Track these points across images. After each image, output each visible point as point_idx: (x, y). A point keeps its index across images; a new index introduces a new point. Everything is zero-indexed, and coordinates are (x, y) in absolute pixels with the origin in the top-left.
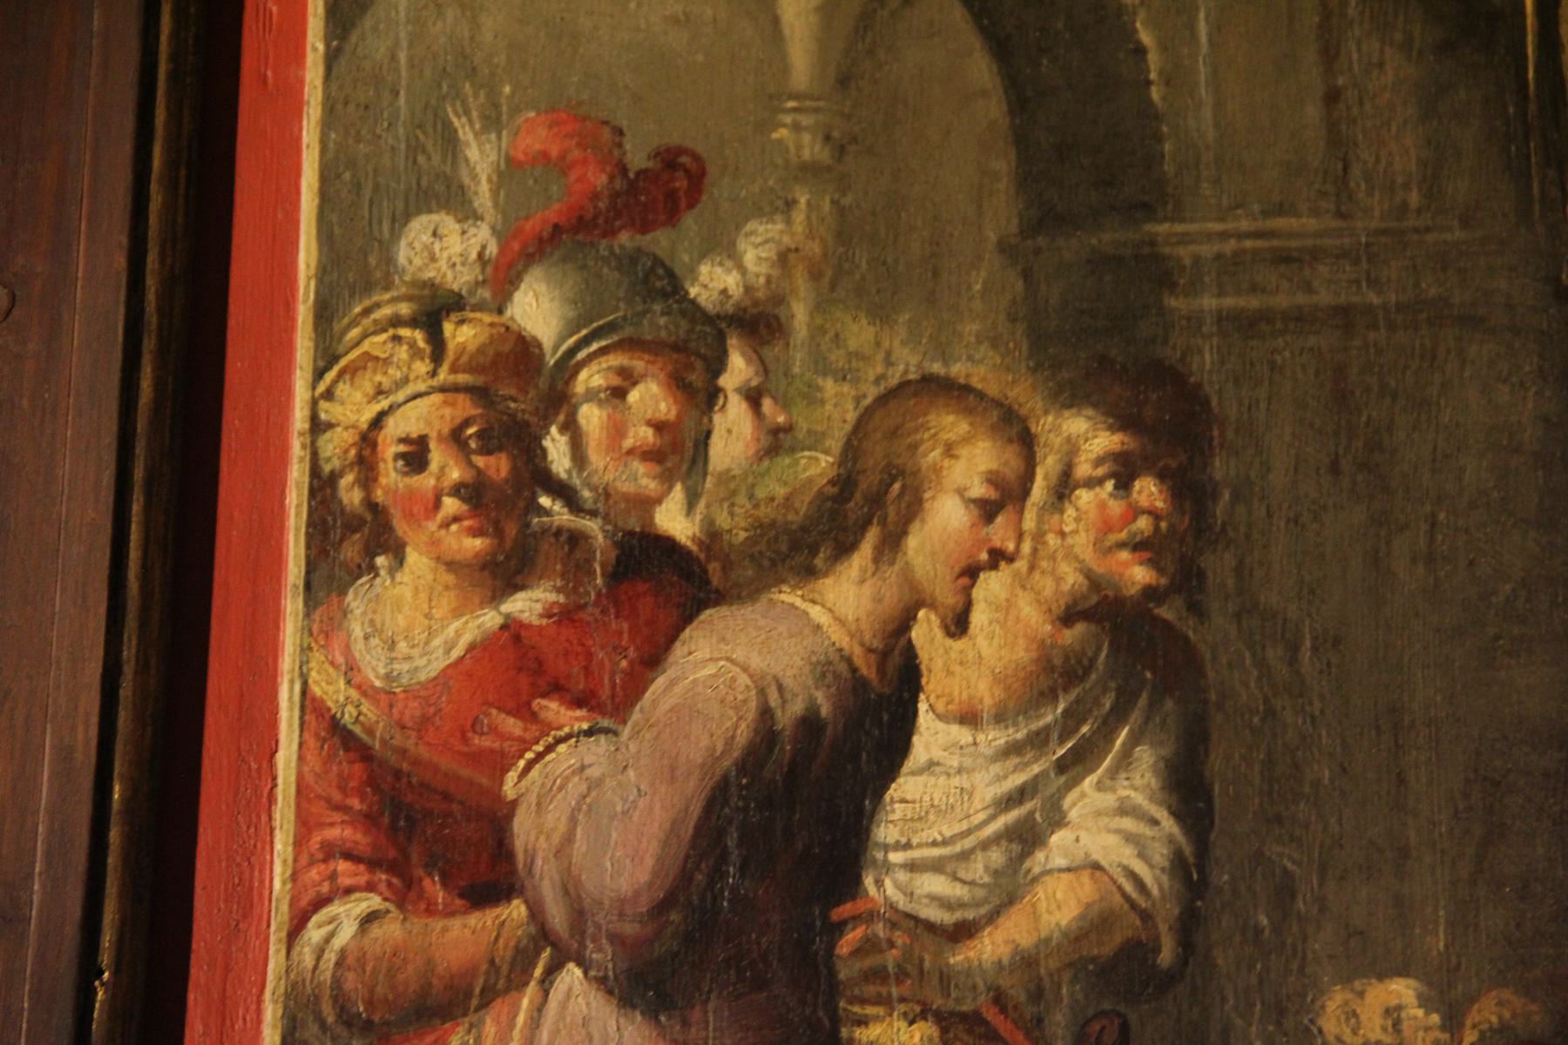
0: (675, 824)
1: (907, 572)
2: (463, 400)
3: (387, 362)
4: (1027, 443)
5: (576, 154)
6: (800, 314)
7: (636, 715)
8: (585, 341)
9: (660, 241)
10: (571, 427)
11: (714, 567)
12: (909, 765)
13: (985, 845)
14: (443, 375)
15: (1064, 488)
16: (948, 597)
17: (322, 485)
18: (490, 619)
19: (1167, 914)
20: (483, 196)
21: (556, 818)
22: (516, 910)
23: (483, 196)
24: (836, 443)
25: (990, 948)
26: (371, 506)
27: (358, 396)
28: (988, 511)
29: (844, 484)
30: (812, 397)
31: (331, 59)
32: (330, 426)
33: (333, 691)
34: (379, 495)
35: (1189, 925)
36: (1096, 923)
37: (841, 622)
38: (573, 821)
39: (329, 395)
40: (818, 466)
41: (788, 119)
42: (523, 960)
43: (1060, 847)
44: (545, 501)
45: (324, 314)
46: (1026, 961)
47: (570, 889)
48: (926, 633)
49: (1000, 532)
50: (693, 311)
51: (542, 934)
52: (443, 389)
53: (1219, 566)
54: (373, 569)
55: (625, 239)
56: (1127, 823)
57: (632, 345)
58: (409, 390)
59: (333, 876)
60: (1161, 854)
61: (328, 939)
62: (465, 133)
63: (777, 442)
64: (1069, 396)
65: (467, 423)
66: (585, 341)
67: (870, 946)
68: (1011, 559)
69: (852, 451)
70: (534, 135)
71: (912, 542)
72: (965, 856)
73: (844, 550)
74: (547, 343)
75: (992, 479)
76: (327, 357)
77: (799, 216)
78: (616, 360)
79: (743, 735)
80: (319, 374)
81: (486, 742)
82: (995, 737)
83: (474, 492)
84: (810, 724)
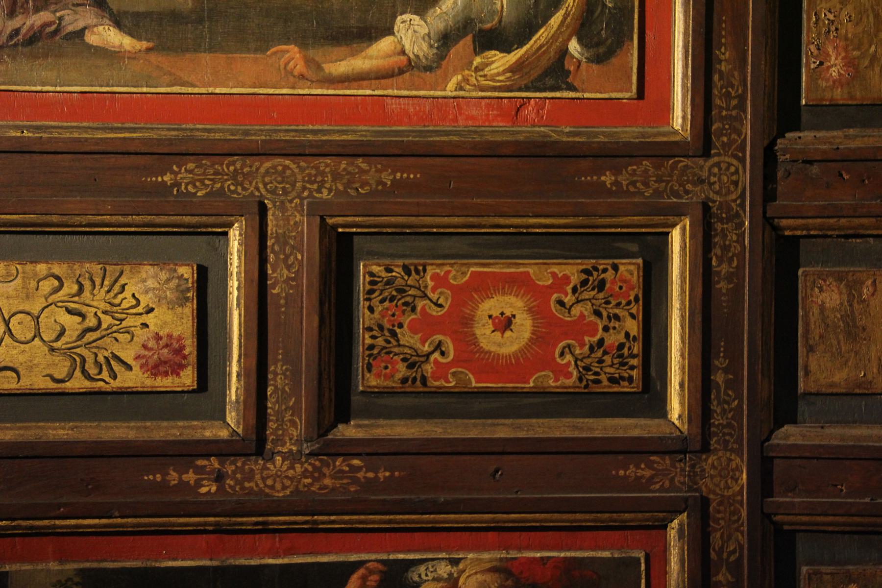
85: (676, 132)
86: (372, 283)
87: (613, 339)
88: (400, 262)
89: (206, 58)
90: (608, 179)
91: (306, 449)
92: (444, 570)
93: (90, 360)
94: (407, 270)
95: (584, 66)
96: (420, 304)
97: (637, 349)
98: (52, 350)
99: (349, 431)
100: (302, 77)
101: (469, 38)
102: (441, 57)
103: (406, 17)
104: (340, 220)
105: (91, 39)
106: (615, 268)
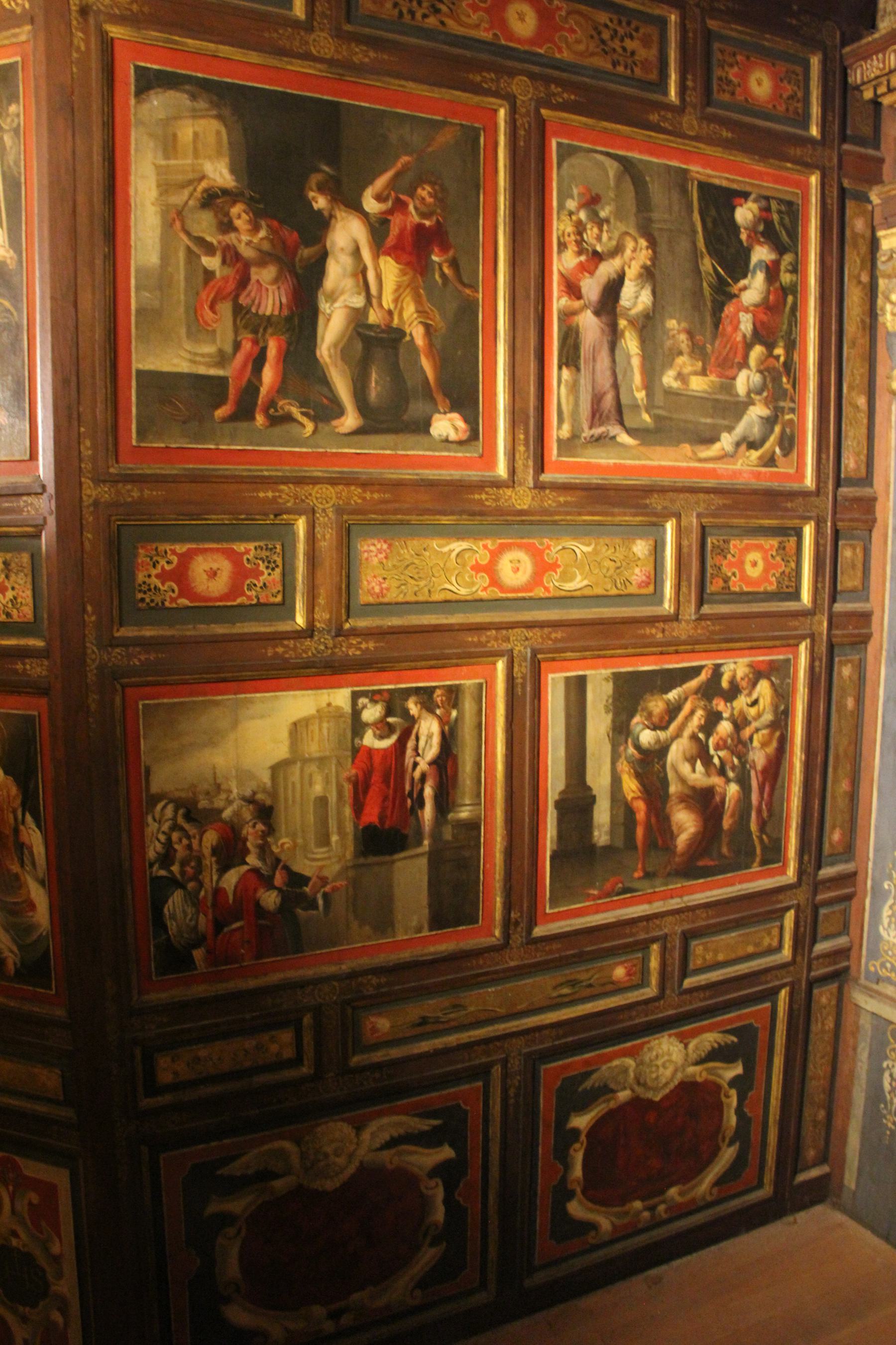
6: (612, 220)
15: (641, 249)
22: (582, 302)
23: (576, 197)
35: (654, 311)
36: (644, 310)
40: (614, 243)
45: (558, 213)
48: (626, 268)
49: (634, 255)
53: (657, 262)
63: (610, 239)
76: (558, 218)
83: (576, 241)
84: (614, 279)
85: (808, 487)
87: (787, 570)
88: (722, 538)
91: (693, 617)
92: (732, 666)
93: (618, 581)
94: (724, 541)
96: (729, 556)
97: (794, 574)
98: (605, 577)
99: (706, 609)
100: (690, 458)
102: (736, 452)
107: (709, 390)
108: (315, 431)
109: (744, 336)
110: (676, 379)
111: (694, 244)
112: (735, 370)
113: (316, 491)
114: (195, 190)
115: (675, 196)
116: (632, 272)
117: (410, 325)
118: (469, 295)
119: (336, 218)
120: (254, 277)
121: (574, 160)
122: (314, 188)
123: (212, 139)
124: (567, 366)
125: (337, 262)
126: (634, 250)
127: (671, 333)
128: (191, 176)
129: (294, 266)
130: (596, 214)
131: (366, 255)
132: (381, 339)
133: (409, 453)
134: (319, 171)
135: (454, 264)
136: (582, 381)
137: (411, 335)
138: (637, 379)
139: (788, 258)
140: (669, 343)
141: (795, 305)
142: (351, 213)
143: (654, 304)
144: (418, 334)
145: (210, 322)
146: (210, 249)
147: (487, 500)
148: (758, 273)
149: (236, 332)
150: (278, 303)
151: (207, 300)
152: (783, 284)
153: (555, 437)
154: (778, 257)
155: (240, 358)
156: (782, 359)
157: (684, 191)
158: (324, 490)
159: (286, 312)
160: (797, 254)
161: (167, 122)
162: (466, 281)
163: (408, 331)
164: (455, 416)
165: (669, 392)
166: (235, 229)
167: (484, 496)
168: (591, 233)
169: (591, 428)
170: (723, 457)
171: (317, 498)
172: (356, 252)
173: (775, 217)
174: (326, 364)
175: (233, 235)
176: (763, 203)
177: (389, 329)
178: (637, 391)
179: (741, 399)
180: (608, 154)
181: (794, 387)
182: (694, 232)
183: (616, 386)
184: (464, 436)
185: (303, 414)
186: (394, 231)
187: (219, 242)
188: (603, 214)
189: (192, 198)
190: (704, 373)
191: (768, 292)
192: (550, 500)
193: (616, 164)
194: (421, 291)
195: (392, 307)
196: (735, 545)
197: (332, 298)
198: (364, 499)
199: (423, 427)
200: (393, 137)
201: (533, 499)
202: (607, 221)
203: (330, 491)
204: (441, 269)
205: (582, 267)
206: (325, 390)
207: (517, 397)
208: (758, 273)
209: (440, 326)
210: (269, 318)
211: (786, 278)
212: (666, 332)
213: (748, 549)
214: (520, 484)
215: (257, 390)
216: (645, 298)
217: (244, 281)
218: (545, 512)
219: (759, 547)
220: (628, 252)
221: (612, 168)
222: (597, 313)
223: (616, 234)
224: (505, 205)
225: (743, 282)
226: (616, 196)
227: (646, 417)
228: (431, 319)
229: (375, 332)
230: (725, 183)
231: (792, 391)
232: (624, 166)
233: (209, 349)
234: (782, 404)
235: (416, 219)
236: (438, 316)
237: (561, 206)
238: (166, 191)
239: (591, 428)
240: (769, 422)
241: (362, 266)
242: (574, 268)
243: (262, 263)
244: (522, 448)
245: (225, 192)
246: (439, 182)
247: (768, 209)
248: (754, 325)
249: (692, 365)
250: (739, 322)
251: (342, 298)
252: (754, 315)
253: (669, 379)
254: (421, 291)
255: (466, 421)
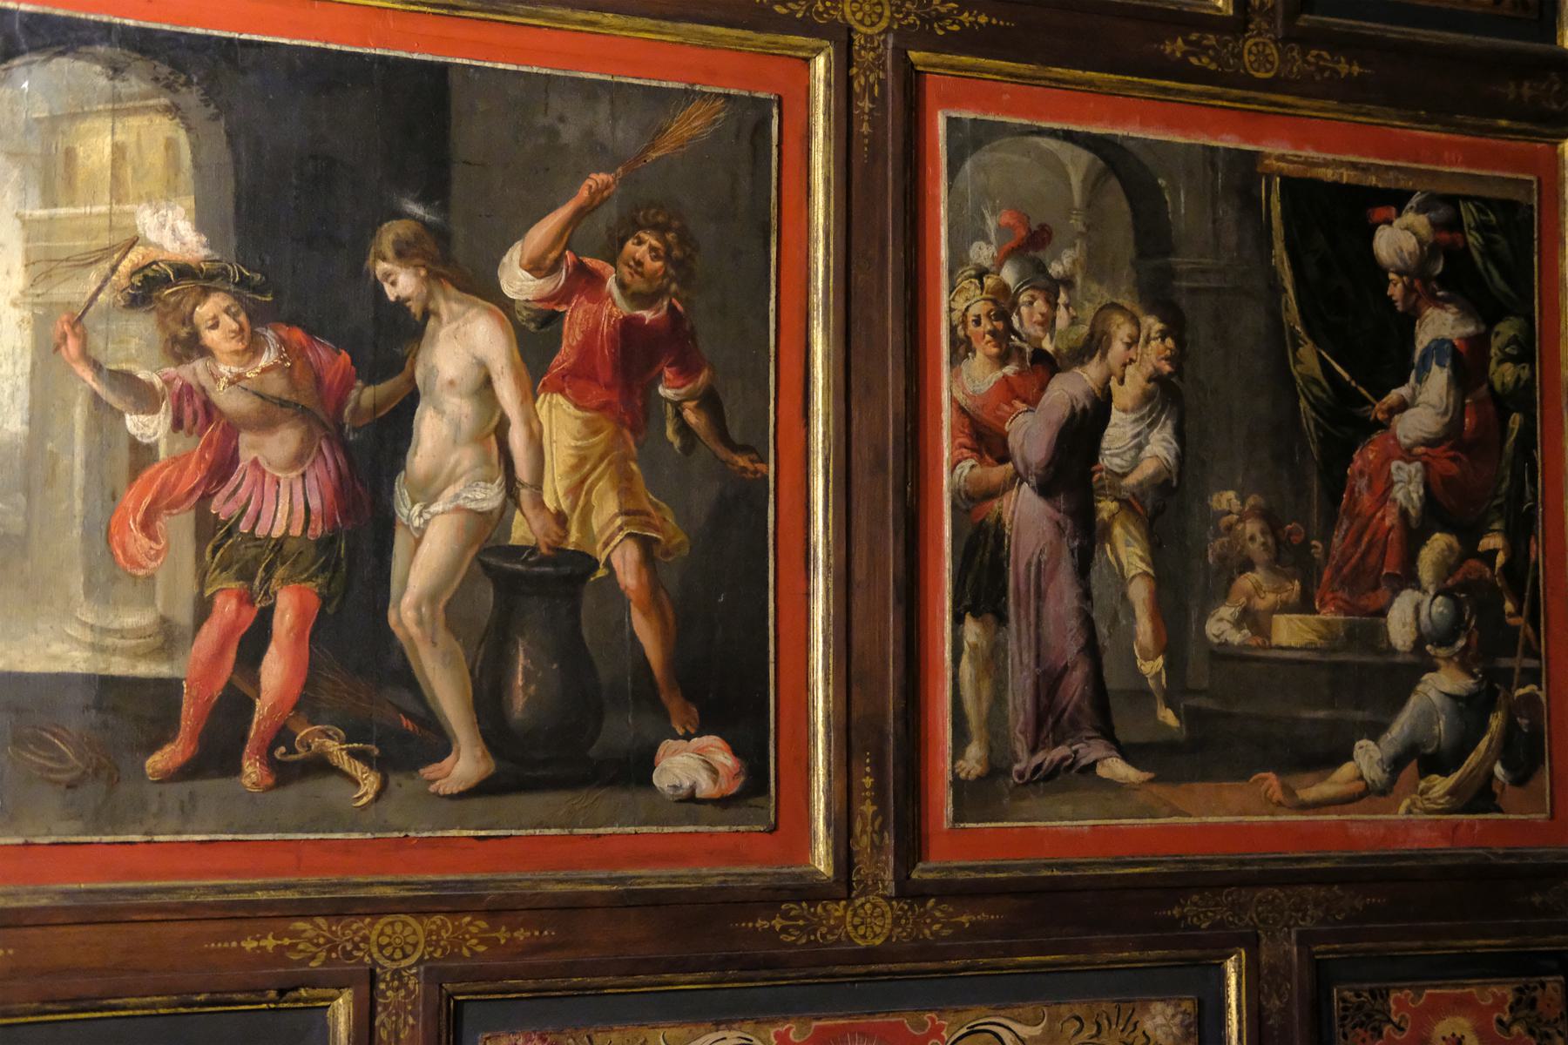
0: (1050, 442)
1: (1108, 365)
2: (990, 303)
3: (969, 289)
4: (1138, 325)
5: (1018, 224)
6: (1078, 280)
7: (1039, 406)
8: (1022, 286)
9: (1041, 254)
10: (1019, 314)
11: (1058, 360)
12: (1110, 424)
13: (1129, 449)
14: (984, 295)
15: (1147, 341)
16: (1119, 373)
17: (953, 330)
18: (999, 374)
19: (1174, 471)
20: (993, 237)
21: (1019, 437)
22: (1010, 465)
23: (993, 237)
24: (1089, 323)
25: (1131, 480)
26: (966, 335)
27: (962, 301)
28: (1129, 346)
29: (1091, 335)
30: (1082, 307)
31: (950, 188)
32: (954, 310)
33: (960, 396)
34: (968, 333)
35: (1180, 475)
36: (1157, 474)
37: (1091, 379)
38: (1024, 439)
39: (953, 300)
40: (1084, 330)
41: (1074, 217)
42: (1013, 480)
43: (1148, 450)
44: (1013, 337)
45: (951, 272)
46: (1140, 484)
47: (1024, 460)
48: (1113, 383)
50: (1050, 278)
51: (1017, 474)
52: (984, 299)
54: (968, 357)
55: (1031, 253)
56: (1164, 444)
57: (1033, 288)
58: (975, 299)
59: (962, 453)
60: (1173, 452)
61: (961, 473)
62: (987, 216)
63: (1074, 321)
64: (1150, 311)
65: (991, 310)
66: (1022, 286)
67: (1101, 479)
68: (1134, 361)
69: (1093, 326)
70: (1006, 218)
71: (1109, 355)
72: (1124, 452)
73: (1092, 357)
74: (1012, 287)
75: (1130, 337)
76: (952, 289)
77: (1078, 249)
78: (1030, 292)
79: (1067, 414)
80: (951, 293)
81: (999, 413)
82: (1132, 417)
83: (993, 333)
84: (1084, 409)
86: (1345, 1009)
88: (1367, 986)
89: (1198, 787)
90: (1537, 899)
94: (1372, 992)
95: (1508, 788)
96: (1387, 1029)
100: (1279, 804)
101: (1415, 762)
102: (1392, 781)
103: (1363, 742)
104: (1322, 947)
105: (1102, 771)
106: (1543, 985)
107: (1320, 643)
108: (379, 796)
109: (1404, 513)
110: (1238, 624)
111: (1275, 316)
112: (1384, 593)
113: (378, 930)
114: (114, 269)
115: (1228, 212)
116: (1126, 394)
117: (606, 544)
118: (744, 469)
119: (437, 315)
120: (246, 456)
121: (985, 156)
122: (390, 254)
123: (155, 157)
124: (976, 615)
125: (440, 412)
126: (1132, 343)
127: (1225, 520)
128: (104, 241)
129: (341, 428)
130: (1041, 268)
131: (507, 392)
132: (541, 577)
133: (601, 831)
134: (399, 215)
135: (710, 402)
136: (1012, 646)
137: (608, 563)
138: (1144, 628)
139: (1507, 329)
140: (1214, 548)
141: (1528, 433)
142: (474, 304)
143: (1181, 458)
144: (625, 564)
145: (141, 558)
146: (145, 398)
147: (784, 929)
148: (1435, 368)
149: (202, 577)
150: (300, 508)
151: (136, 510)
152: (1498, 386)
153: (950, 778)
154: (1483, 328)
155: (210, 633)
156: (1500, 559)
157: (1249, 200)
158: (398, 927)
159: (317, 529)
160: (1530, 319)
161: (54, 122)
162: (735, 434)
163: (602, 558)
164: (711, 741)
165: (1222, 655)
166: (206, 352)
167: (778, 923)
168: (1029, 314)
169: (1033, 751)
170: (1367, 793)
171: (381, 948)
172: (485, 387)
173: (1474, 239)
174: (411, 639)
175: (199, 365)
176: (1443, 212)
177: (560, 554)
178: (1146, 659)
179: (1399, 659)
180: (1068, 136)
181: (1534, 619)
182: (1276, 289)
183: (1092, 649)
184: (729, 786)
185: (353, 754)
186: (572, 336)
187: (168, 382)
188: (1056, 269)
189: (107, 289)
190: (1305, 605)
191: (1460, 411)
192: (938, 921)
193: (1084, 156)
194: (634, 467)
195: (565, 505)
196: (1401, 1000)
197: (427, 492)
198: (493, 943)
199: (638, 769)
200: (569, 134)
201: (896, 921)
202: (1067, 282)
203: (413, 929)
204: (679, 414)
205: (1008, 389)
206: (406, 700)
207: (855, 689)
208: (1435, 368)
209: (676, 541)
210: (280, 543)
211: (1504, 374)
212: (1215, 517)
213: (1437, 1010)
214: (863, 893)
215: (251, 706)
216: (1160, 447)
217: (223, 467)
218: (924, 950)
219: (1462, 1005)
220: (1118, 348)
221: (1078, 163)
222: (1045, 490)
223: (1089, 311)
224: (827, 267)
225: (1394, 395)
226: (1088, 227)
227: (1168, 717)
228: (657, 530)
229: (524, 562)
230: (1346, 176)
231: (1530, 630)
232: (1104, 158)
233: (135, 619)
234: (1504, 662)
235: (623, 308)
236: (670, 520)
237: (958, 259)
238: (48, 275)
239: (1033, 751)
240: (1471, 709)
241: (496, 419)
242: (988, 392)
243: (265, 424)
244: (869, 809)
245: (184, 272)
246: (676, 224)
247: (1455, 224)
248: (1427, 486)
249: (1276, 591)
250: (1390, 485)
251: (450, 492)
252: (1426, 465)
253: (1221, 626)
254: (634, 467)
255: (736, 752)
